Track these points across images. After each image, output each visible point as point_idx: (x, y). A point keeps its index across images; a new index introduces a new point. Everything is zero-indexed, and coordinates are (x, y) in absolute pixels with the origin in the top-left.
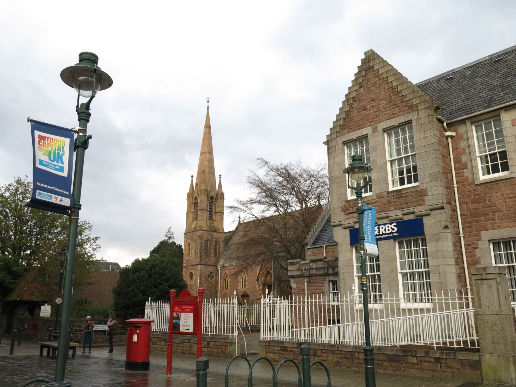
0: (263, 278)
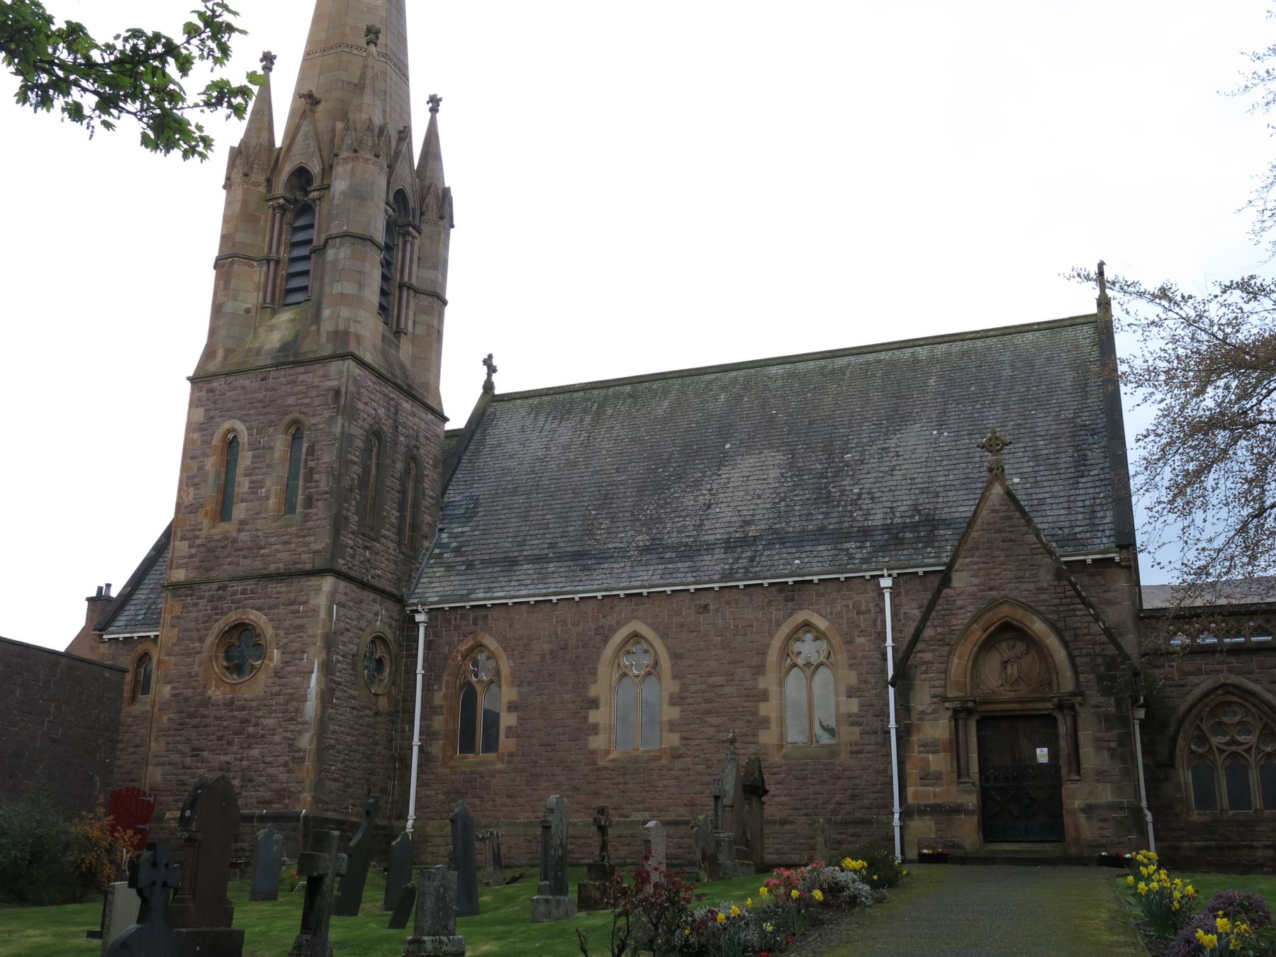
0: (958, 664)
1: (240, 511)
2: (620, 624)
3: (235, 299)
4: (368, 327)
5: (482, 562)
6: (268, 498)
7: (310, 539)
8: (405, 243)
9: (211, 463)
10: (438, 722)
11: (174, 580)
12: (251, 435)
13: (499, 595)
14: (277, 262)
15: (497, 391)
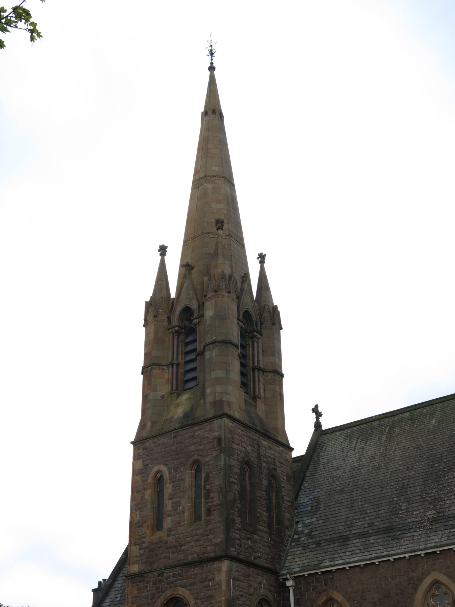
1: (168, 523)
2: (424, 575)
3: (155, 390)
4: (235, 396)
5: (326, 541)
6: (183, 512)
7: (211, 536)
8: (253, 343)
9: (148, 494)
11: (132, 572)
12: (170, 473)
13: (339, 563)
14: (178, 365)
15: (324, 428)
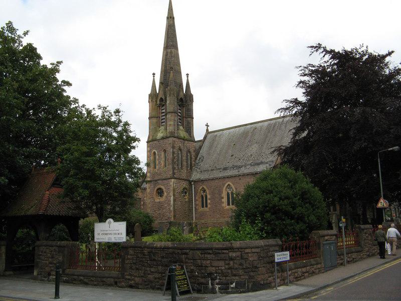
1: (157, 167)
10: (197, 202)
